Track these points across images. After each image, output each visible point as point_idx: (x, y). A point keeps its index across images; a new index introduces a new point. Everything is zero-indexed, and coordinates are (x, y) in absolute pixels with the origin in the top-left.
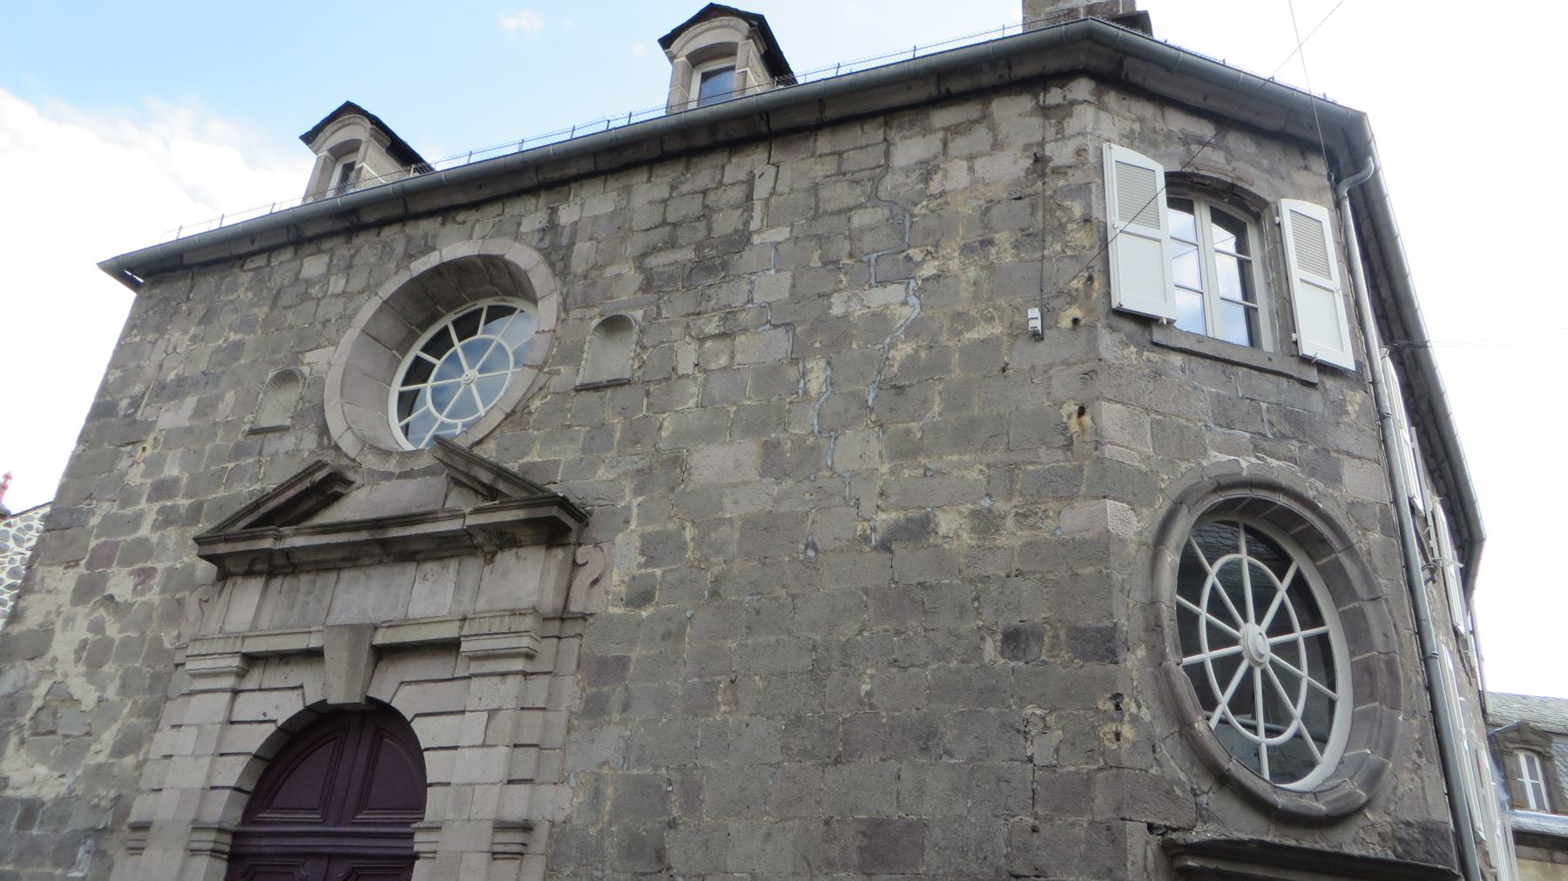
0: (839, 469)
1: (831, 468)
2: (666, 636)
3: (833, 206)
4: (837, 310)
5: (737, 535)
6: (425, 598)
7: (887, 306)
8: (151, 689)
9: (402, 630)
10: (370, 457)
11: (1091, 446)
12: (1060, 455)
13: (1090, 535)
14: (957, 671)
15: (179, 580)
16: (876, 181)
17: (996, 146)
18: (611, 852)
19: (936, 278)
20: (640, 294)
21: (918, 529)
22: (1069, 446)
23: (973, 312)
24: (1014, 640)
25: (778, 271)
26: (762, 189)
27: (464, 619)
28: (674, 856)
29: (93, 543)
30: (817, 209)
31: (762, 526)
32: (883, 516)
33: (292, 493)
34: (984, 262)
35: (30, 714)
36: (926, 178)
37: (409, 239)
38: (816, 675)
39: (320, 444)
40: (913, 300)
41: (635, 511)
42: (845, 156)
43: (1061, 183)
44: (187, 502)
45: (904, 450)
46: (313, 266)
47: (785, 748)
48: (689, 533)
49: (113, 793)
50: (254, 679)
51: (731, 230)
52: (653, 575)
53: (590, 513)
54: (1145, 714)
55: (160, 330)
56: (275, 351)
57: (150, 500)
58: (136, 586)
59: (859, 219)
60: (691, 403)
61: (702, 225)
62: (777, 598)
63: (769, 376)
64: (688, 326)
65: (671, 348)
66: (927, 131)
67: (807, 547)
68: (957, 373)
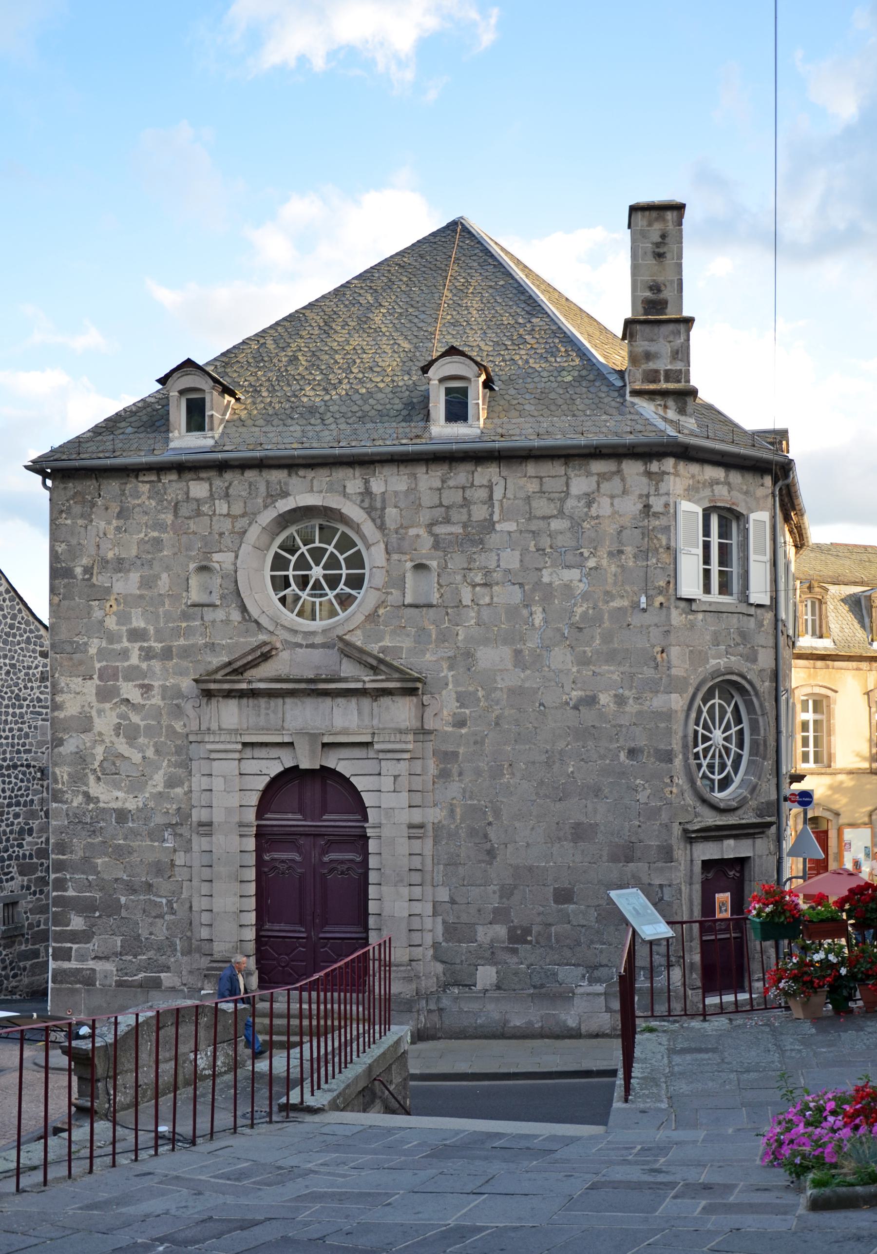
0: (553, 668)
1: (549, 667)
2: (476, 743)
3: (539, 513)
4: (546, 579)
5: (505, 696)
6: (345, 718)
7: (571, 581)
8: (178, 752)
9: (338, 736)
10: (282, 631)
11: (666, 668)
12: (652, 671)
13: (664, 710)
14: (609, 764)
15: (173, 694)
16: (563, 501)
17: (625, 492)
18: (462, 833)
19: (596, 568)
20: (433, 551)
21: (591, 701)
22: (656, 667)
23: (614, 592)
24: (632, 753)
25: (512, 550)
26: (498, 494)
27: (374, 733)
28: (492, 835)
29: (98, 665)
30: (531, 513)
31: (516, 692)
32: (574, 693)
33: (250, 658)
34: (619, 563)
35: (97, 764)
36: (589, 505)
37: (268, 482)
38: (548, 764)
39: (244, 618)
40: (584, 579)
41: (450, 679)
42: (544, 480)
43: (657, 523)
44: (160, 645)
45: (583, 661)
46: (199, 489)
47: (537, 794)
48: (480, 694)
49: (174, 807)
50: (248, 753)
51: (482, 518)
52: (465, 713)
53: (426, 677)
54: (681, 782)
55: (87, 517)
56: (188, 549)
57: (129, 640)
58: (142, 695)
59: (556, 525)
60: (473, 622)
61: (464, 510)
62: (528, 728)
63: (512, 612)
64: (465, 576)
65: (457, 588)
66: (589, 474)
67: (540, 705)
68: (607, 625)
